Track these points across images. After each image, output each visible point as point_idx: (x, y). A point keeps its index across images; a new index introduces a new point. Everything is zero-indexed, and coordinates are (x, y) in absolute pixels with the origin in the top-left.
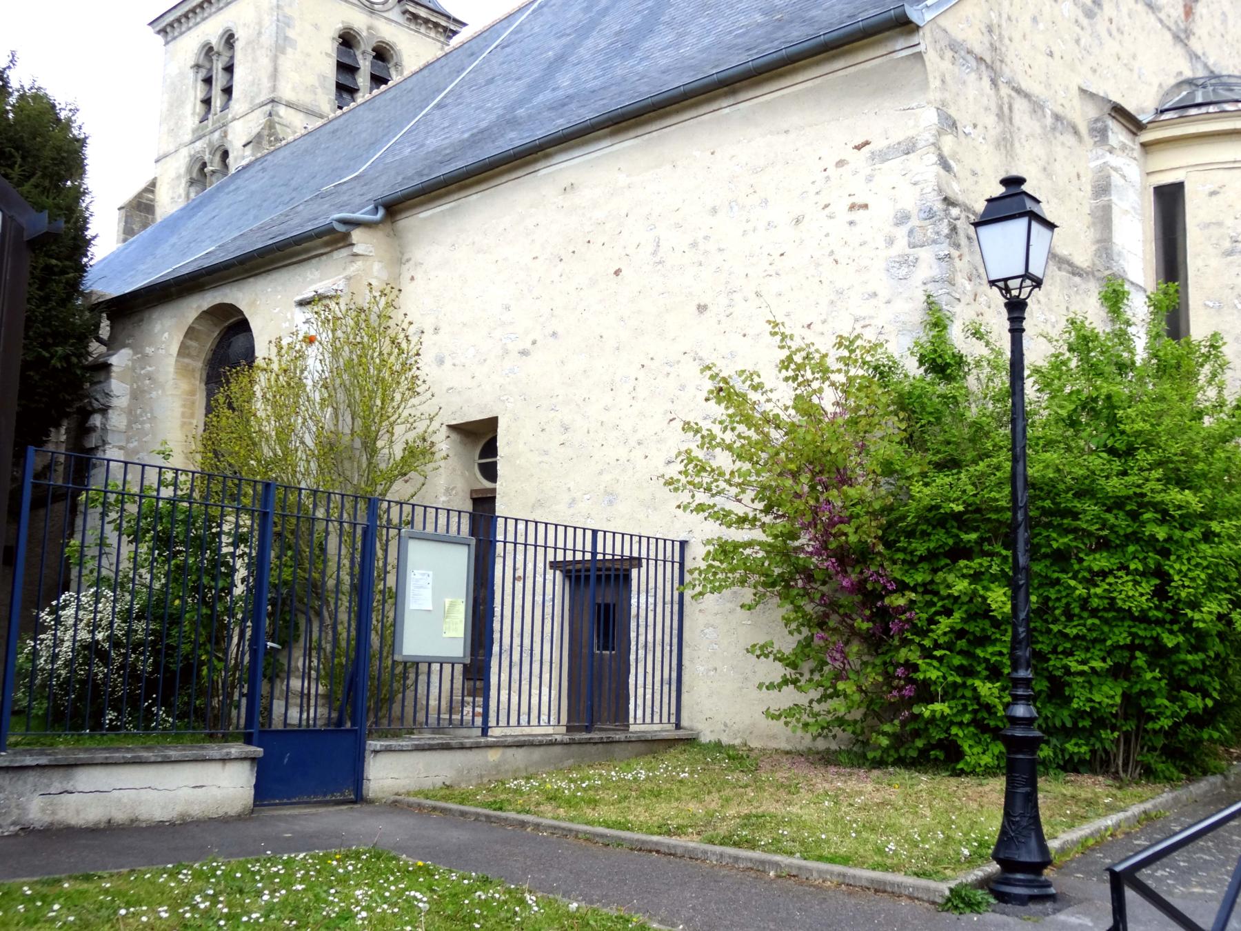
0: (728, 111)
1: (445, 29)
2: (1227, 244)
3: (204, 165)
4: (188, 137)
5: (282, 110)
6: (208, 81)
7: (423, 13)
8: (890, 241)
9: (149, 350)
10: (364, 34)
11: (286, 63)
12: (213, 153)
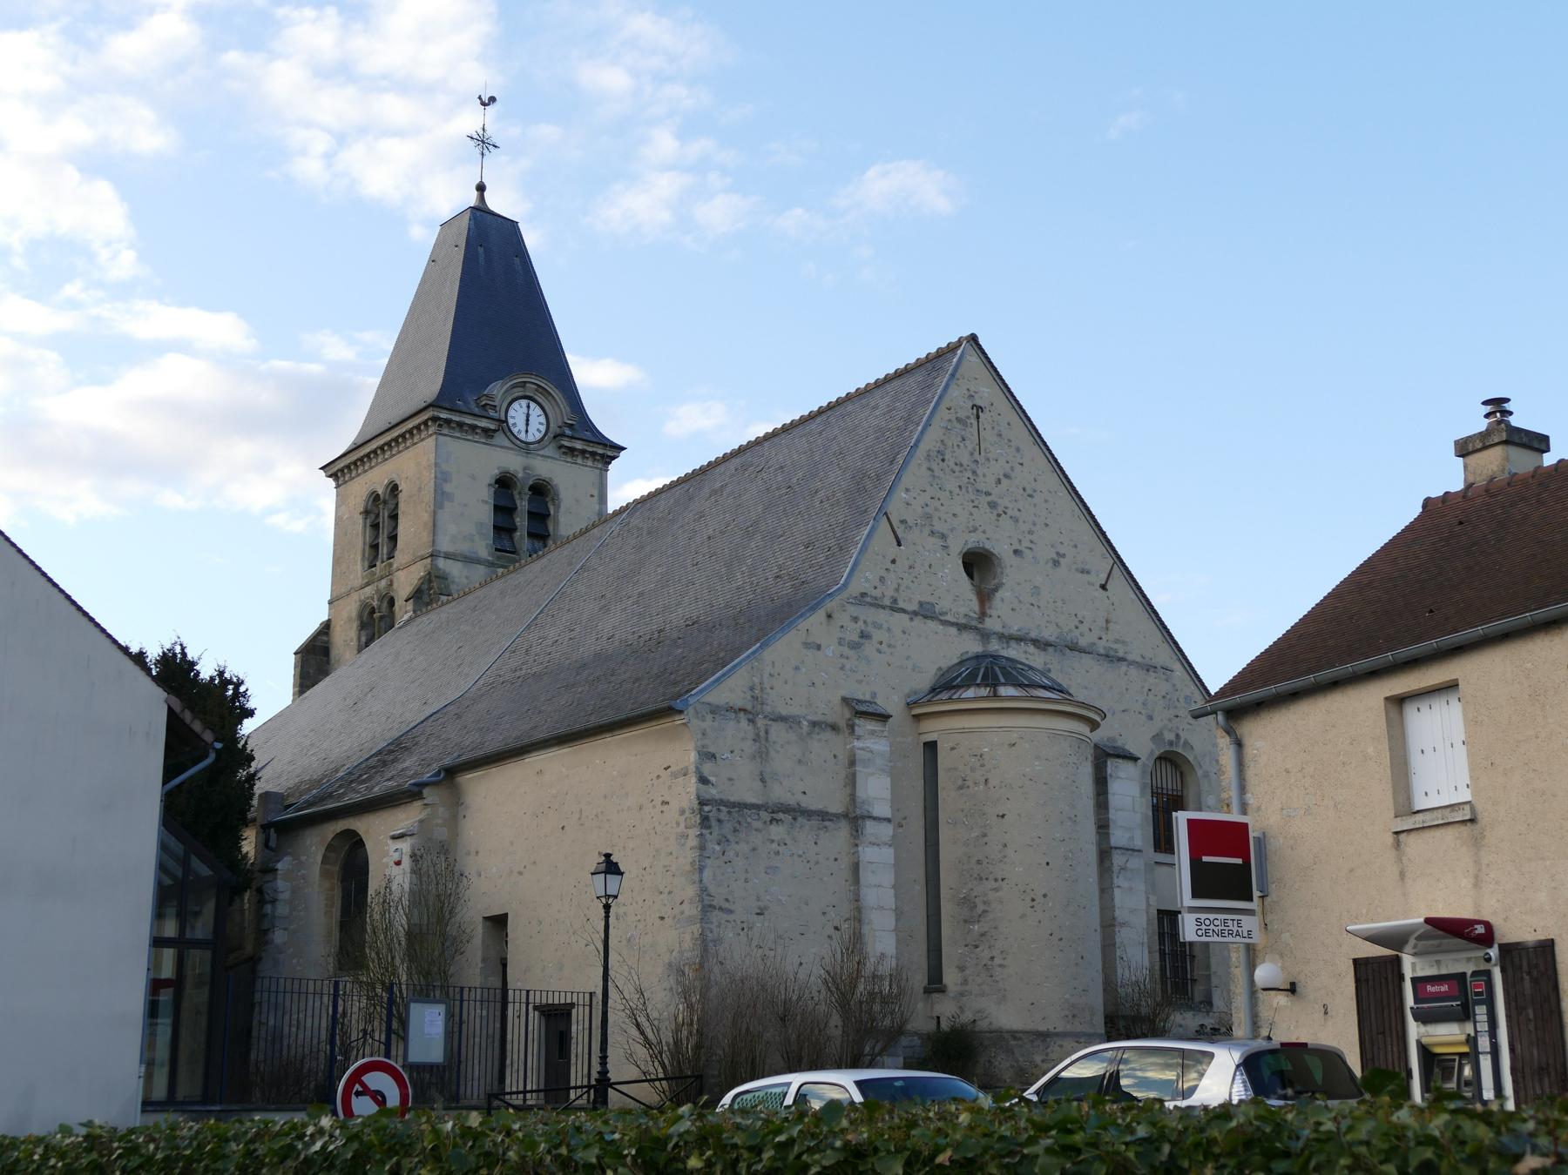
0: (610, 740)
1: (602, 456)
2: (960, 782)
3: (373, 611)
4: (359, 582)
5: (441, 563)
6: (375, 526)
7: (579, 445)
8: (678, 824)
9: (303, 858)
10: (520, 475)
11: (443, 516)
12: (381, 599)
